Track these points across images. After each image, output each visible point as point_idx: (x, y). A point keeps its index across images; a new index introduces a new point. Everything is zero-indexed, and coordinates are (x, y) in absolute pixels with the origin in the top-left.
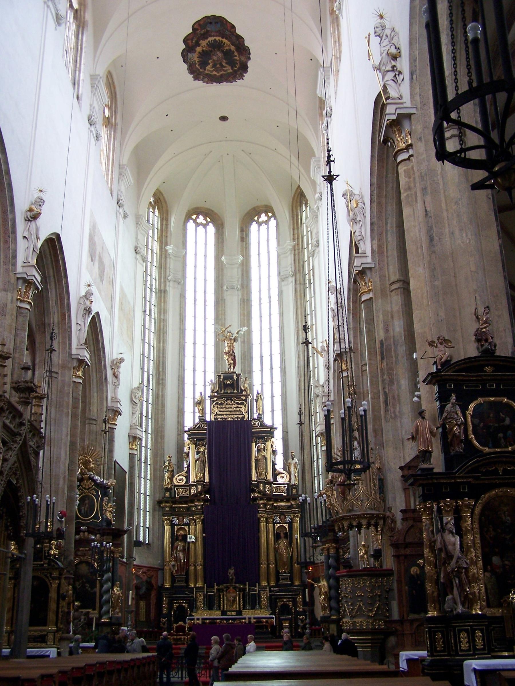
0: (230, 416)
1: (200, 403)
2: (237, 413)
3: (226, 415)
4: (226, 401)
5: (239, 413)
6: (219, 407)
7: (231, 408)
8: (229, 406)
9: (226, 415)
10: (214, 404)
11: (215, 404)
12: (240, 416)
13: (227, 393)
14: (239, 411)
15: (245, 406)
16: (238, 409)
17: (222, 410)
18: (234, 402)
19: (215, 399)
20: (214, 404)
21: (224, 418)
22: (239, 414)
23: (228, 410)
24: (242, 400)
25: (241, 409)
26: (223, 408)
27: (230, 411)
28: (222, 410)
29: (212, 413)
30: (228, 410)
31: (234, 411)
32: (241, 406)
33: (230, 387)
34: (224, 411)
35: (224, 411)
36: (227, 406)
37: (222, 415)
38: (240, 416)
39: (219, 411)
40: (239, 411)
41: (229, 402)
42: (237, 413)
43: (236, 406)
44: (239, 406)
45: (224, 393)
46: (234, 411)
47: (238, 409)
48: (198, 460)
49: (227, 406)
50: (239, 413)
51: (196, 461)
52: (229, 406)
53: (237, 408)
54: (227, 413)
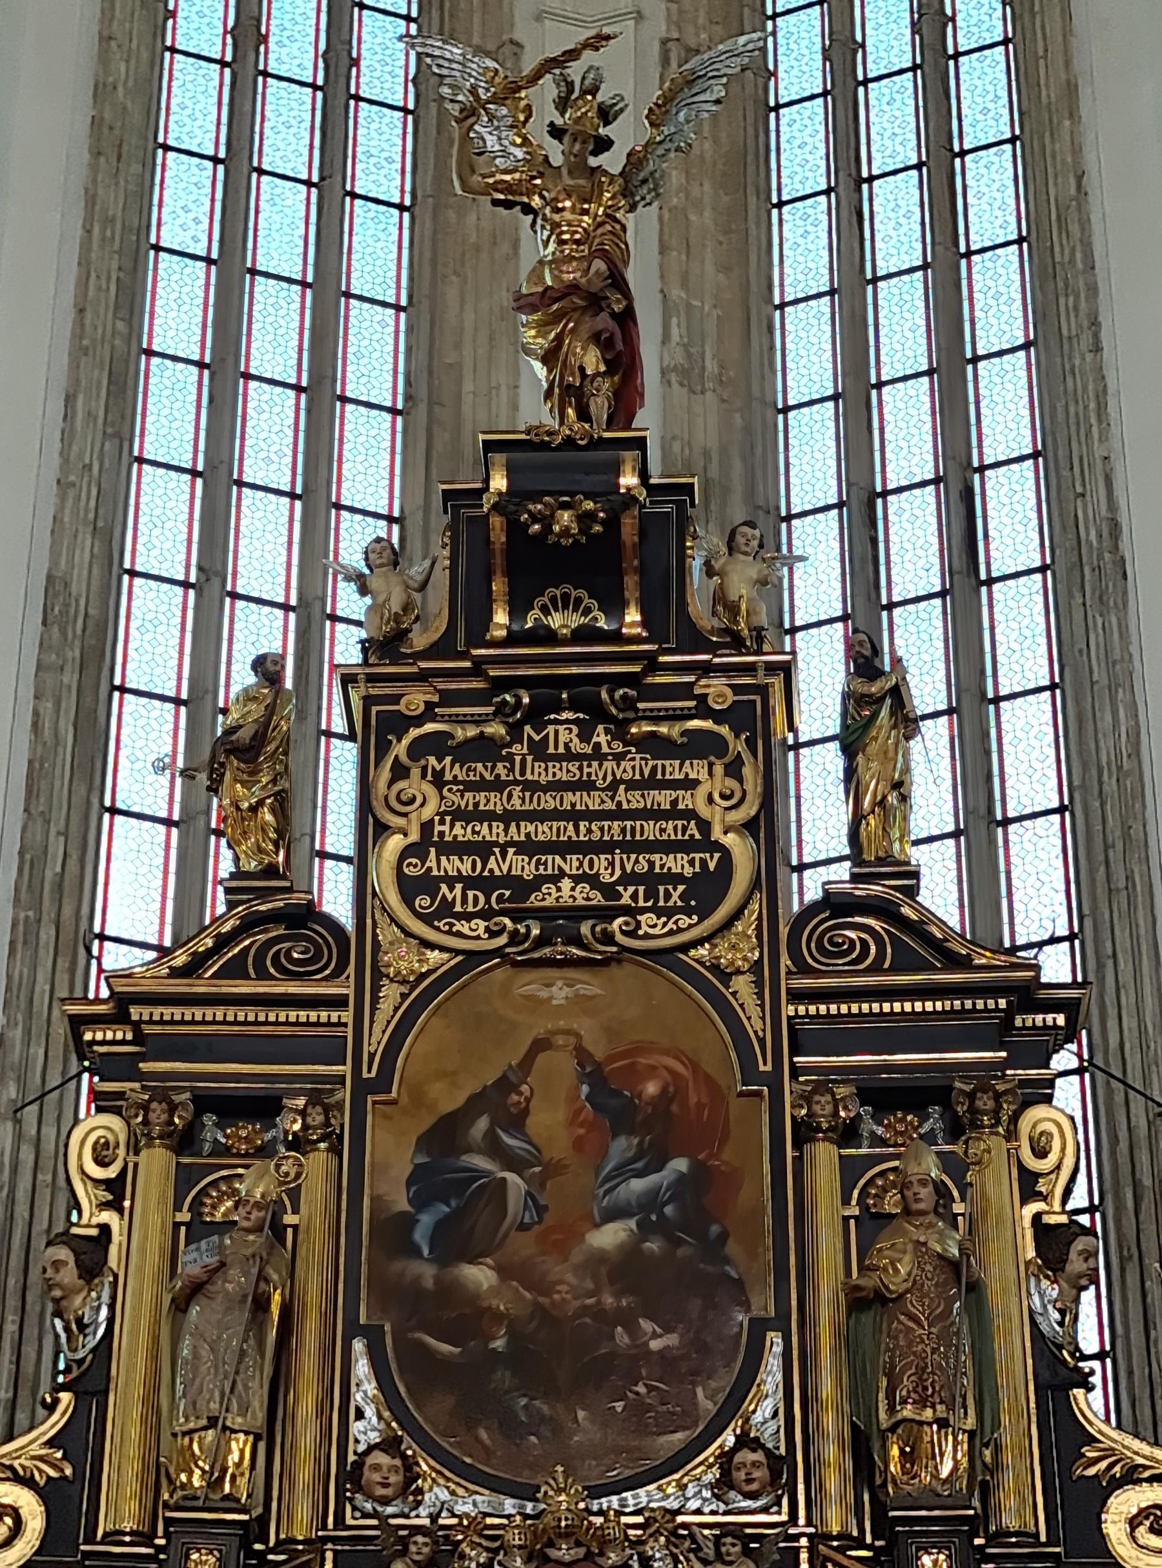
0: (572, 863)
1: (243, 753)
2: (650, 830)
3: (528, 848)
4: (537, 715)
5: (670, 829)
6: (454, 771)
7: (588, 786)
8: (565, 772)
9: (528, 848)
10: (400, 749)
11: (418, 749)
12: (677, 863)
13: (548, 637)
14: (673, 813)
15: (734, 769)
16: (663, 798)
17: (493, 802)
18: (619, 731)
19: (415, 699)
20: (400, 749)
21: (509, 880)
22: (669, 847)
23: (549, 802)
24: (703, 710)
25: (696, 801)
26: (498, 786)
27: (574, 816)
28: (493, 802)
29: (370, 827)
30: (549, 802)
31: (619, 814)
32: (696, 770)
33: (573, 577)
34: (509, 817)
35: (509, 817)
36: (538, 772)
37: (483, 850)
38: (677, 863)
39: (458, 815)
40: (673, 813)
41: (563, 734)
42: (650, 830)
43: (635, 765)
44: (673, 769)
45: (512, 639)
46: (619, 814)
47: (663, 798)
48: (196, 1289)
49: (538, 772)
50: (670, 829)
51: (181, 1305)
52: (565, 772)
53: (651, 783)
54: (544, 832)
